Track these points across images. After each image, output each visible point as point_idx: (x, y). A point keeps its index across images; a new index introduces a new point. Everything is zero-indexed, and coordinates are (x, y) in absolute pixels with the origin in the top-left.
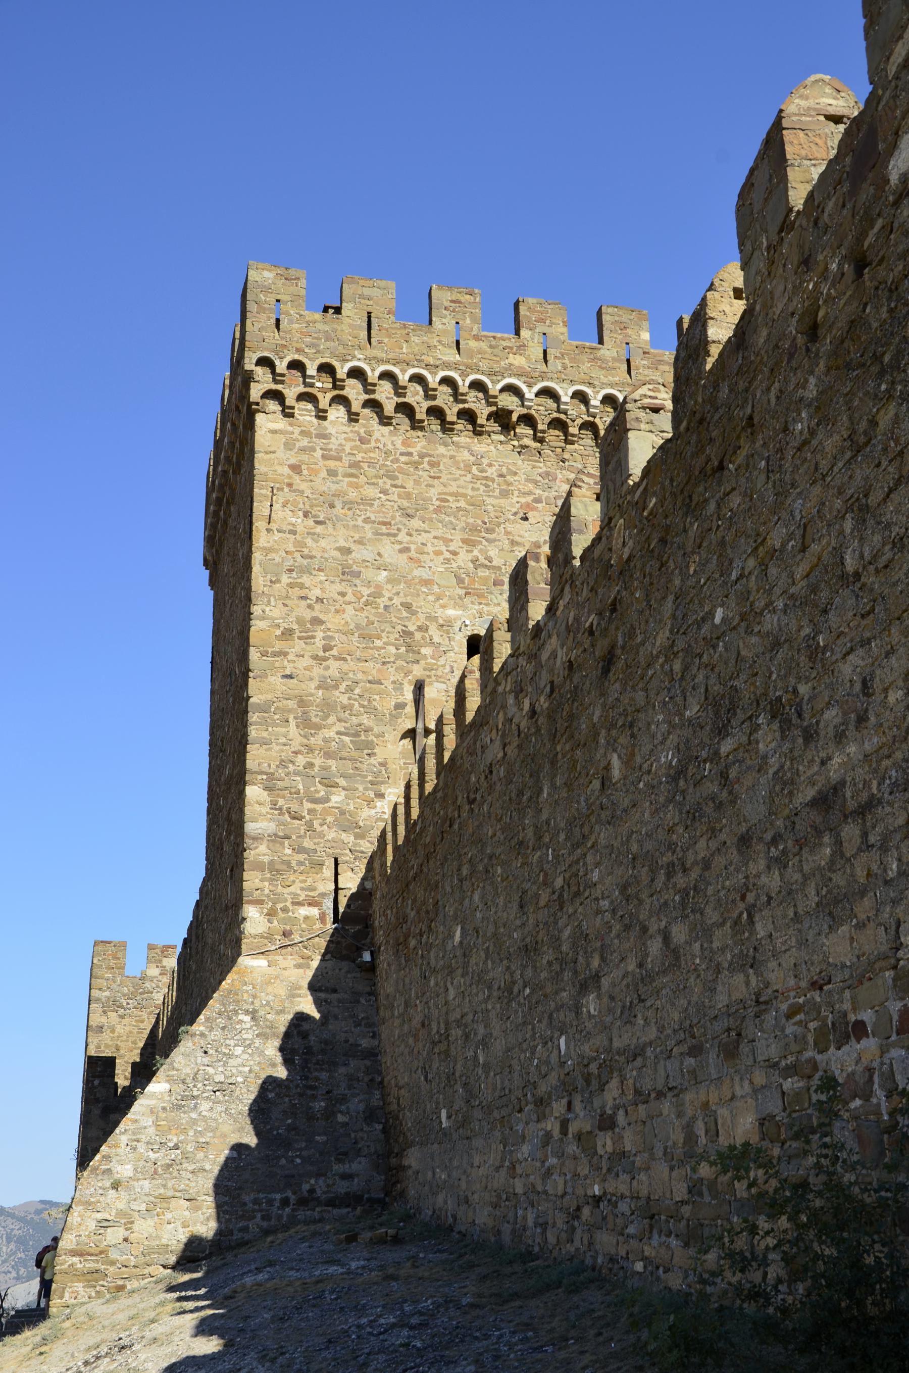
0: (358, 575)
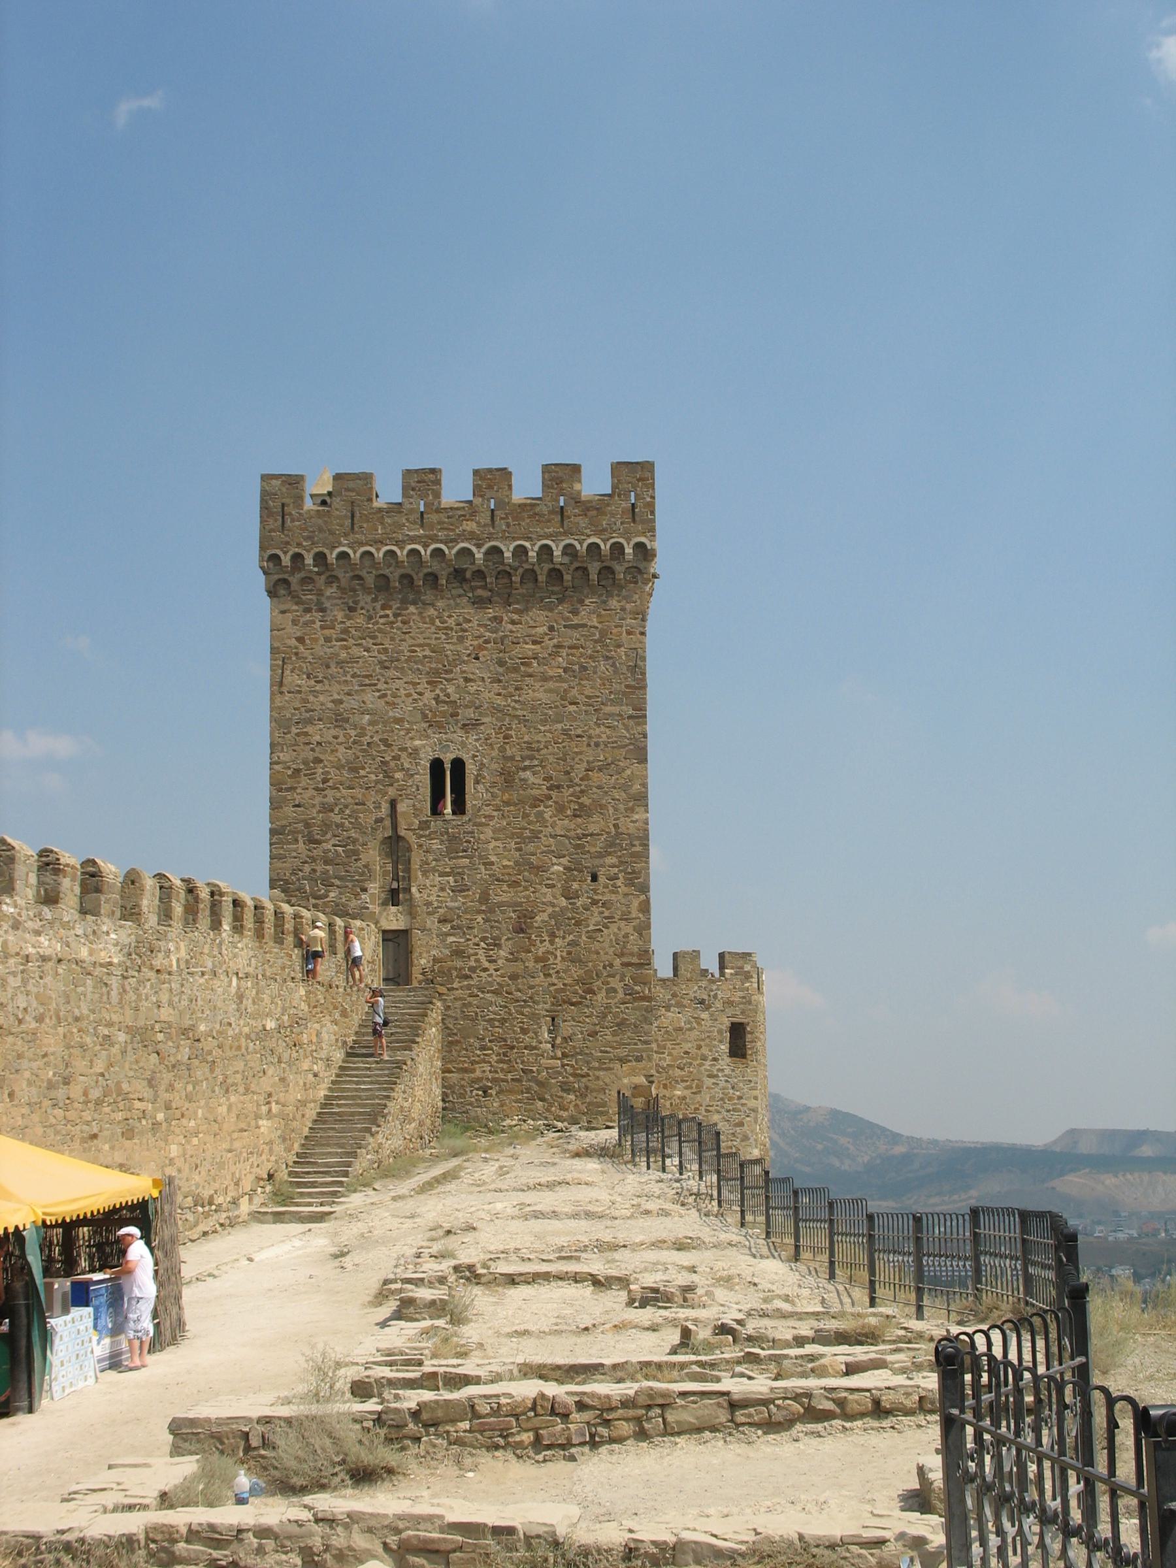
0: (347, 720)
